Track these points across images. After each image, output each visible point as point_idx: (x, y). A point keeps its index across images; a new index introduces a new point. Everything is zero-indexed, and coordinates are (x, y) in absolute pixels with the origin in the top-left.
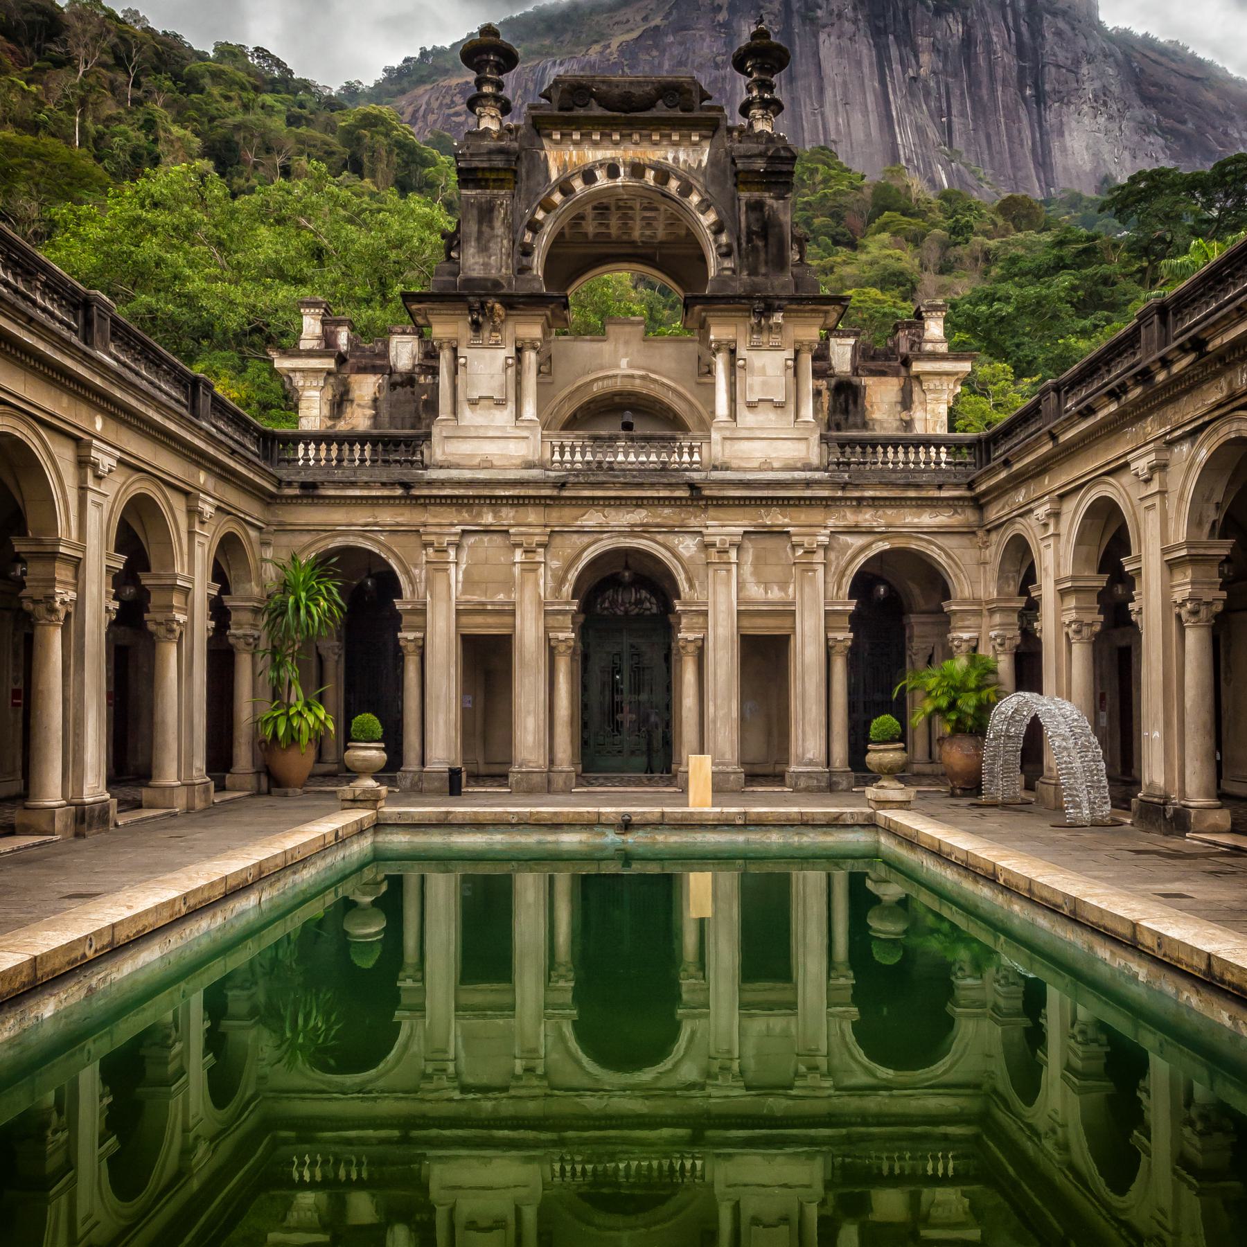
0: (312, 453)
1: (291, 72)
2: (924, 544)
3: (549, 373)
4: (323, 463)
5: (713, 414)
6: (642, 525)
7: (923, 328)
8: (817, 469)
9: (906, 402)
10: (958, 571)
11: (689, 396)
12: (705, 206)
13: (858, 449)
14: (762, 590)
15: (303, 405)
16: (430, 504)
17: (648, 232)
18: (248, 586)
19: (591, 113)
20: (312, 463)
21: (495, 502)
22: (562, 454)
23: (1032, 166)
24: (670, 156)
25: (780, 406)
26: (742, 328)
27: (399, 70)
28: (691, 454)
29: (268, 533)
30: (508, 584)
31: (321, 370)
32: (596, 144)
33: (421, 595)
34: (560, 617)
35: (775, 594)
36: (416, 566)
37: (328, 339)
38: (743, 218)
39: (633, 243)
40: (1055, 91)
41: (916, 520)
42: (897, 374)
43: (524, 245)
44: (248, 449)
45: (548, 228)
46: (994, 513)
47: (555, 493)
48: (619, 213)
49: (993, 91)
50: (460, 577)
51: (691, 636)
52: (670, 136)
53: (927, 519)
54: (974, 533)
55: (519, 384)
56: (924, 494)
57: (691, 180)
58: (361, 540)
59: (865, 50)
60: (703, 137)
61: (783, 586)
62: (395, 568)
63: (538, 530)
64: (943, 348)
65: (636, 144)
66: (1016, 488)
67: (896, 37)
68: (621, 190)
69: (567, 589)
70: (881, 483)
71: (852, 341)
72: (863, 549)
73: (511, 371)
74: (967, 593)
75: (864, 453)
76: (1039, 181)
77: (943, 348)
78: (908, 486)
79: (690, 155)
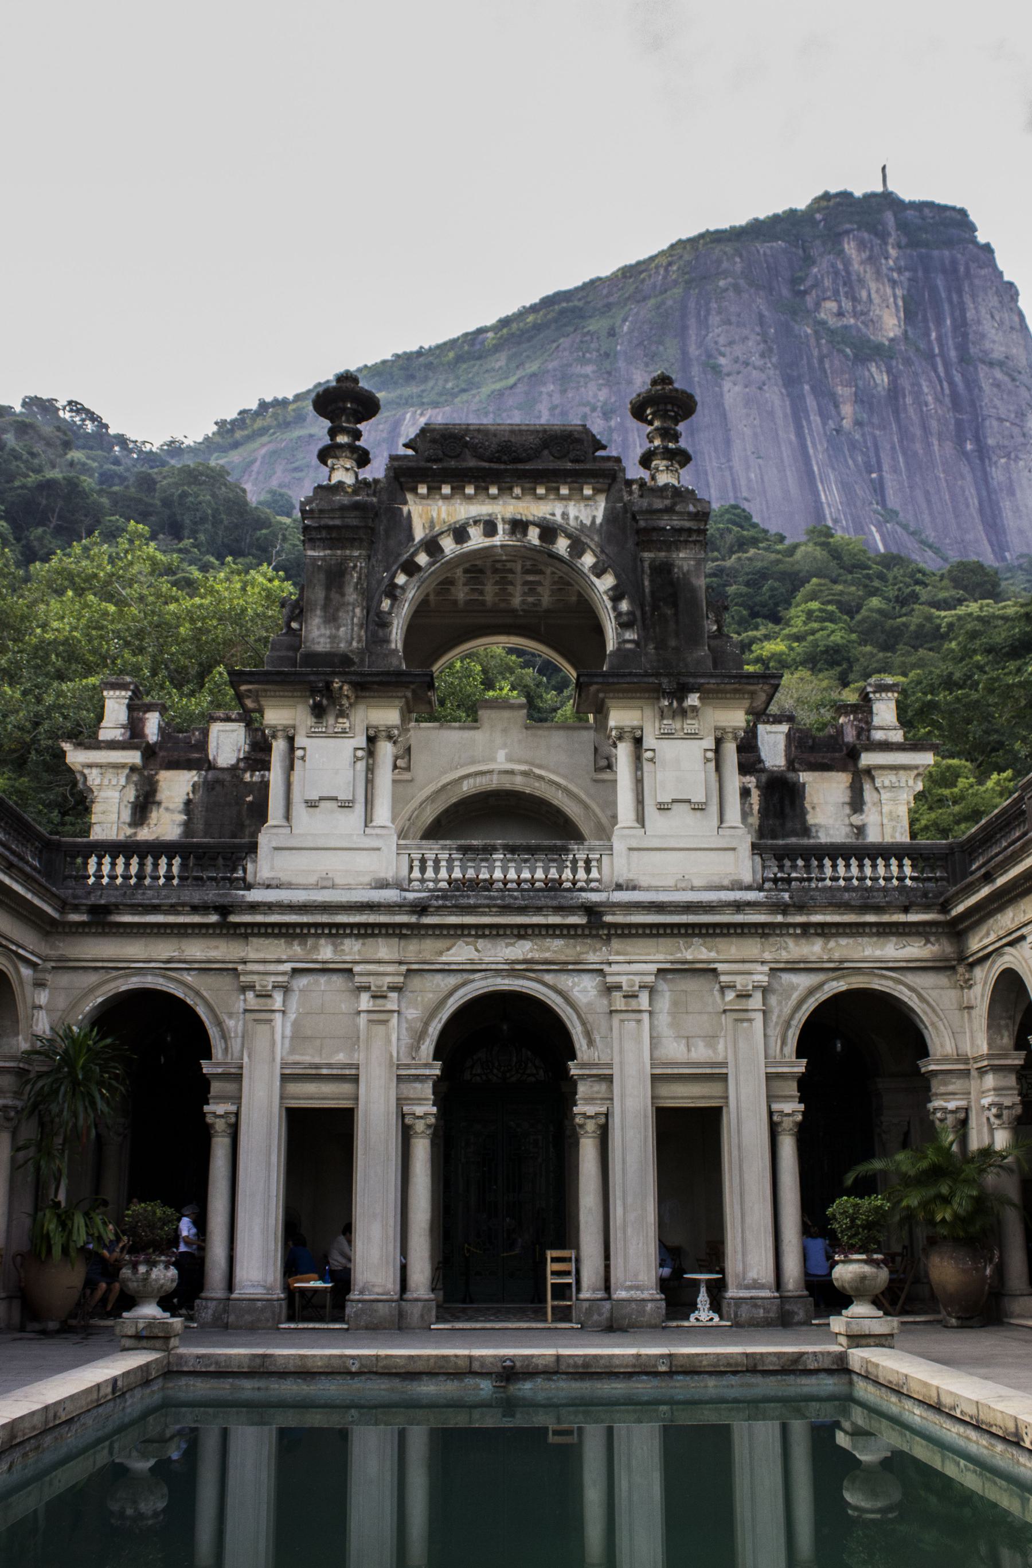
0: (106, 869)
1: (106, 426)
2: (890, 983)
3: (408, 769)
4: (119, 881)
5: (614, 818)
6: (525, 962)
7: (871, 712)
8: (749, 888)
9: (857, 804)
10: (935, 1019)
11: (584, 796)
12: (599, 571)
13: (800, 863)
14: (683, 1048)
15: (96, 808)
16: (254, 935)
17: (530, 599)
18: (13, 1041)
19: (464, 465)
20: (105, 881)
21: (336, 932)
22: (423, 869)
23: (981, 528)
24: (558, 512)
25: (699, 808)
26: (648, 712)
27: (233, 422)
28: (588, 870)
29: (45, 970)
30: (353, 1040)
31: (123, 766)
32: (469, 498)
33: (236, 1054)
34: (418, 1085)
35: (701, 1053)
36: (230, 1015)
37: (135, 727)
38: (647, 583)
39: (514, 611)
40: (999, 447)
41: (878, 953)
42: (844, 769)
43: (379, 613)
44: (27, 862)
45: (410, 594)
46: (976, 944)
47: (413, 919)
48: (497, 577)
49: (929, 445)
50: (288, 1032)
51: (590, 1110)
52: (558, 489)
53: (892, 950)
54: (953, 968)
55: (370, 782)
56: (886, 918)
57: (584, 539)
58: (161, 981)
60: (597, 491)
61: (711, 1039)
62: (204, 1017)
63: (390, 968)
64: (897, 736)
65: (518, 498)
66: (1001, 909)
67: (813, 389)
68: (499, 550)
69: (427, 1048)
70: (831, 905)
71: (784, 728)
72: (811, 992)
73: (361, 766)
74: (949, 1048)
75: (807, 867)
76: (991, 545)
77: (897, 736)
78: (865, 908)
79: (583, 511)
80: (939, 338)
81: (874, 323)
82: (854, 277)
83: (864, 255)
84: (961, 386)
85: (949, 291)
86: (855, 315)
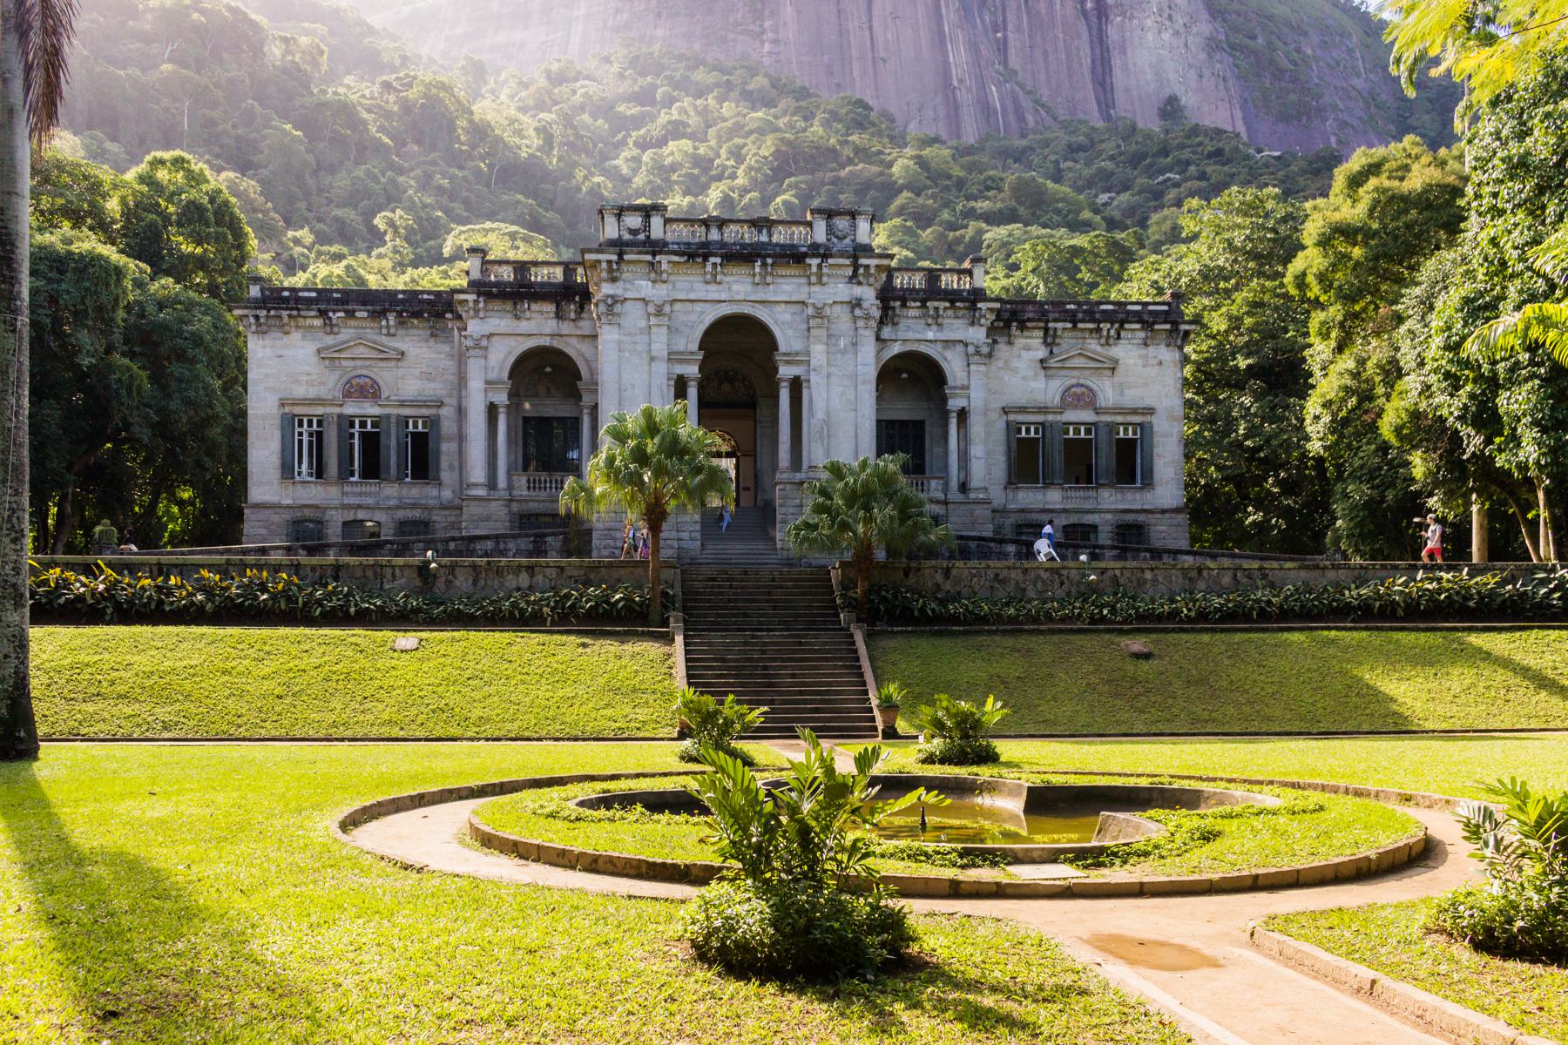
76: (1099, 103)
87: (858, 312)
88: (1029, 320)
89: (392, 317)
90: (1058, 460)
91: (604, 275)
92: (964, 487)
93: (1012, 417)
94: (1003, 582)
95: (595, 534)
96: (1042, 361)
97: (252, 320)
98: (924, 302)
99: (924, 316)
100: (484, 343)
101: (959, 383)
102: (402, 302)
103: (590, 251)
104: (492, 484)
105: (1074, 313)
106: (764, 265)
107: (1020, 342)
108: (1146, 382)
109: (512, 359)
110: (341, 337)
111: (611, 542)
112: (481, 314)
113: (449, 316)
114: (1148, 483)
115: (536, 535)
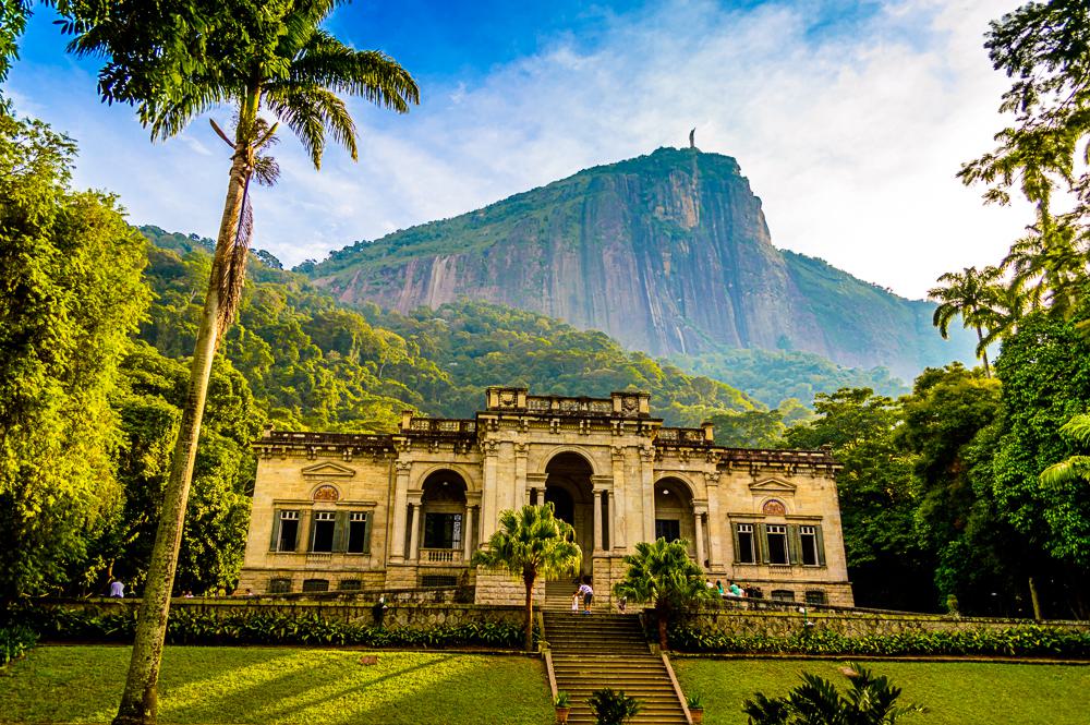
23: (735, 329)
27: (340, 252)
49: (708, 285)
59: (629, 256)
67: (649, 252)
80: (717, 228)
81: (683, 218)
82: (674, 194)
83: (679, 183)
84: (728, 255)
85: (723, 203)
86: (673, 214)
87: (642, 452)
88: (740, 460)
89: (350, 450)
90: (765, 548)
91: (489, 427)
92: (707, 564)
93: (733, 520)
94: (751, 625)
95: (477, 589)
96: (750, 485)
97: (263, 451)
98: (677, 447)
99: (677, 456)
100: (409, 466)
101: (701, 498)
102: (357, 441)
103: (482, 413)
104: (406, 556)
105: (767, 456)
106: (585, 424)
107: (735, 474)
108: (814, 498)
109: (425, 477)
110: (318, 462)
111: (487, 595)
112: (408, 449)
113: (386, 450)
114: (823, 566)
115: (437, 590)
